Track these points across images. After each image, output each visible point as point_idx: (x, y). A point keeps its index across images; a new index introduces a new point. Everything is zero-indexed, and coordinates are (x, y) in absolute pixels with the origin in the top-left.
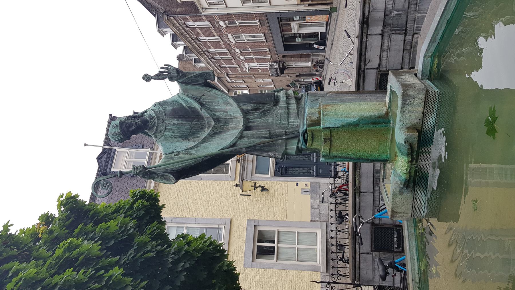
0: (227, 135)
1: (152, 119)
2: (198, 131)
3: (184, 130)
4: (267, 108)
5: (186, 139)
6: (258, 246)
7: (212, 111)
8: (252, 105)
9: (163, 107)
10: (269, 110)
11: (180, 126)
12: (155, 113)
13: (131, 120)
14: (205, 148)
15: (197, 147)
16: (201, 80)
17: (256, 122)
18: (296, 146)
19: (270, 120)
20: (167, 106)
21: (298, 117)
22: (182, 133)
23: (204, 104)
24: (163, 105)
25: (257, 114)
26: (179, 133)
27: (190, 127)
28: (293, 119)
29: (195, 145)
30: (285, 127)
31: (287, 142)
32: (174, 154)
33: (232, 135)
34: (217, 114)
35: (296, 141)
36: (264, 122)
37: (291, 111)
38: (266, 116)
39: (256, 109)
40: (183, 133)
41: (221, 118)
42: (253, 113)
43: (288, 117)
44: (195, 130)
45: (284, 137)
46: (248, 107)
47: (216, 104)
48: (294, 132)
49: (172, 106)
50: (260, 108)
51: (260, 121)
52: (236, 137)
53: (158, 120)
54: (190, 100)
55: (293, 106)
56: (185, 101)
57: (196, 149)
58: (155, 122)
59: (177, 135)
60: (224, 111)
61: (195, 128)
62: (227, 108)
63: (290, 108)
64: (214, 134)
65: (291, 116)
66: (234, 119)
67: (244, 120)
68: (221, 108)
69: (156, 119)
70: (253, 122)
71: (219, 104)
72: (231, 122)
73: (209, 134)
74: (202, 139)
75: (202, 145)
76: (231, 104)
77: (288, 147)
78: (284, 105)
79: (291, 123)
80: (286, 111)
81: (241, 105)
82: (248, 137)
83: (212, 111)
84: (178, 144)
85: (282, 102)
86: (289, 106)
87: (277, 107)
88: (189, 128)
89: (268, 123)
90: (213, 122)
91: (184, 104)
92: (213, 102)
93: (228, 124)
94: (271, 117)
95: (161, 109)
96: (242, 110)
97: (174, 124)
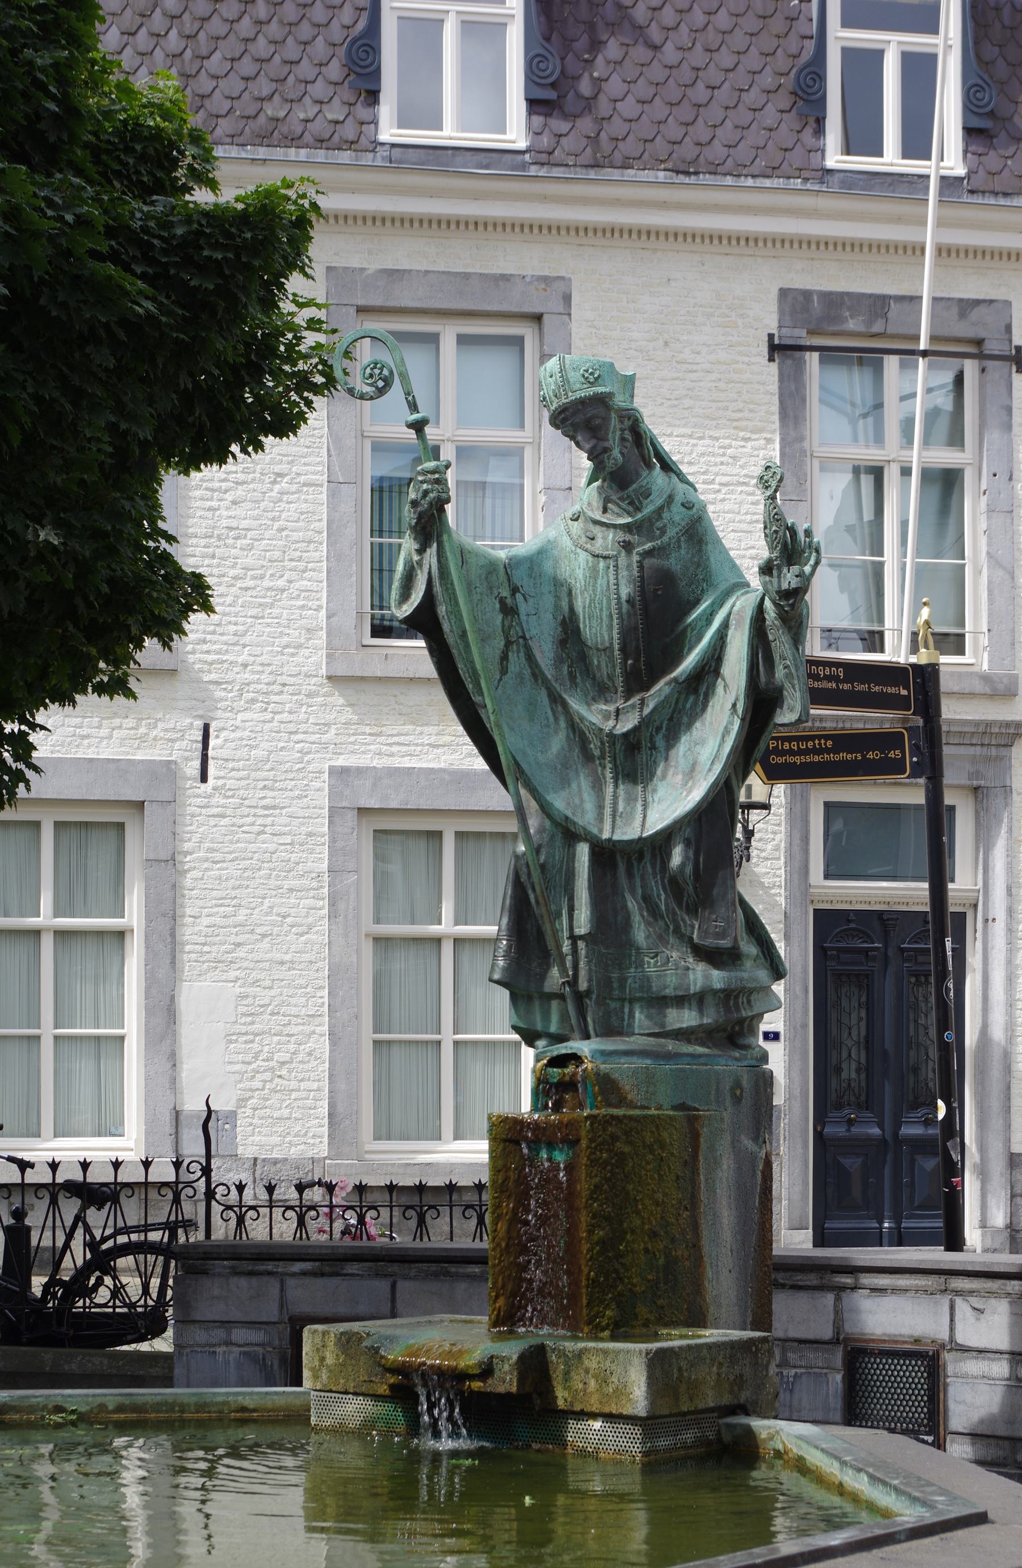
1: (632, 503)
8: (689, 869)
9: (682, 539)
14: (532, 705)
15: (534, 675)
20: (683, 552)
22: (584, 618)
23: (696, 691)
26: (584, 607)
29: (541, 671)
32: (505, 593)
33: (577, 801)
44: (599, 662)
57: (527, 672)
70: (630, 875)
79: (626, 1010)
81: (688, 832)
83: (671, 719)
87: (691, 960)
95: (671, 532)
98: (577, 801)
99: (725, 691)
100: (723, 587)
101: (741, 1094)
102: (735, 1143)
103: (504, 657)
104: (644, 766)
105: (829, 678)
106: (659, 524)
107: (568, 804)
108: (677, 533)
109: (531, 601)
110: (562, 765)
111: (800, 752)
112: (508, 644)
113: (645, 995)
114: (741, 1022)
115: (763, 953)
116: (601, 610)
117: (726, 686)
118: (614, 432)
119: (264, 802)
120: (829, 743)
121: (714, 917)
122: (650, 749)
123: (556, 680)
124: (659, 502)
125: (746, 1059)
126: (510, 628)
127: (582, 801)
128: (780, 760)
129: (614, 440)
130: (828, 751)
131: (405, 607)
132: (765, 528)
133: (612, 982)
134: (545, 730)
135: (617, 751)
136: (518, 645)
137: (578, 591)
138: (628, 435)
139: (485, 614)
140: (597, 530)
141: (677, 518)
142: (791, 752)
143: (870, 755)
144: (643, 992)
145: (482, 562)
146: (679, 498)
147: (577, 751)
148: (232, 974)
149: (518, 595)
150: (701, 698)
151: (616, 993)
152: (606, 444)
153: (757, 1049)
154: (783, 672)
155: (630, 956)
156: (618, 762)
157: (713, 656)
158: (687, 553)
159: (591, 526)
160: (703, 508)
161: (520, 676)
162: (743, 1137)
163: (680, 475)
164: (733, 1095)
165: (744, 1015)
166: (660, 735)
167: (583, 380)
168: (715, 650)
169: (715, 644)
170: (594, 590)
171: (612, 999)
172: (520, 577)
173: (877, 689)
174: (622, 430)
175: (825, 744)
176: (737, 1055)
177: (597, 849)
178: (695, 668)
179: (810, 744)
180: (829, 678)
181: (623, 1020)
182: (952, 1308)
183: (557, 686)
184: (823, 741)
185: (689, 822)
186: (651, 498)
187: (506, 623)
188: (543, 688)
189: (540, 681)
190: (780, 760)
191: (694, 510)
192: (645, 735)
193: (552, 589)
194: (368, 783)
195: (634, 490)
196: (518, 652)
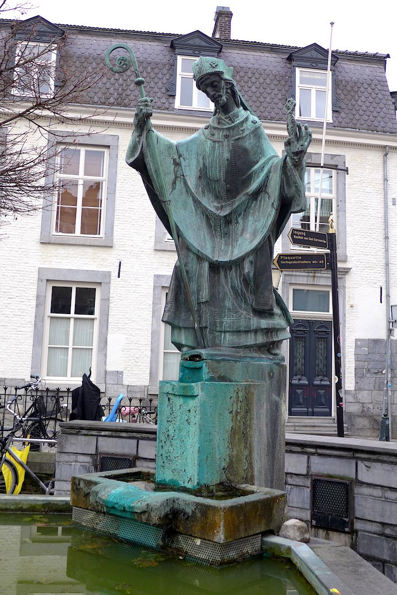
0: (205, 236)
3: (213, 169)
4: (249, 298)
6: (71, 289)
7: (245, 211)
8: (252, 275)
10: (246, 301)
12: (239, 123)
13: (227, 89)
15: (187, 191)
16: (290, 192)
17: (227, 283)
18: (183, 343)
19: (228, 304)
20: (252, 141)
21: (233, 347)
23: (256, 199)
24: (255, 135)
25: (238, 283)
27: (218, 178)
28: (230, 339)
29: (190, 189)
30: (216, 327)
31: (191, 329)
32: (176, 157)
33: (203, 244)
34: (240, 220)
35: (190, 343)
36: (225, 294)
38: (237, 297)
39: (246, 281)
40: (209, 169)
42: (240, 277)
43: (233, 332)
44: (215, 186)
45: (196, 326)
46: (247, 268)
47: (255, 217)
49: (253, 148)
50: (249, 287)
51: (228, 289)
53: (229, 129)
54: (262, 176)
55: (250, 340)
56: (263, 168)
57: (184, 190)
58: (225, 125)
60: (243, 230)
61: (217, 187)
62: (247, 236)
63: (249, 334)
64: (207, 216)
65: (234, 337)
66: (230, 246)
68: (249, 225)
69: (230, 126)
70: (226, 277)
73: (207, 209)
75: (191, 199)
76: (252, 241)
77: (183, 331)
78: (253, 326)
79: (223, 336)
80: (242, 329)
81: (251, 258)
83: (245, 211)
84: (194, 162)
85: (259, 323)
86: (253, 334)
87: (252, 315)
88: (216, 178)
89: (223, 300)
90: (225, 214)
91: (256, 167)
92: (259, 213)
94: (233, 304)
96: (244, 259)
100: (269, 156)
101: (273, 375)
102: (269, 397)
103: (174, 183)
105: (301, 236)
106: (242, 129)
109: (187, 161)
110: (197, 228)
111: (291, 260)
112: (176, 177)
113: (231, 330)
114: (273, 343)
115: (283, 313)
116: (216, 164)
117: (269, 197)
119: (135, 284)
120: (300, 258)
121: (262, 296)
124: (242, 119)
125: (275, 359)
127: (206, 244)
128: (284, 262)
130: (300, 260)
133: (216, 324)
134: (191, 214)
136: (181, 178)
138: (229, 91)
139: (167, 164)
140: (216, 132)
141: (249, 127)
142: (288, 260)
143: (313, 262)
144: (230, 328)
148: (124, 332)
149: (181, 158)
152: (220, 94)
153: (280, 355)
154: (294, 189)
155: (225, 312)
156: (222, 228)
164: (269, 375)
166: (240, 218)
168: (265, 182)
171: (216, 331)
172: (182, 150)
173: (316, 240)
174: (227, 89)
176: (271, 358)
177: (211, 266)
178: (256, 189)
179: (294, 258)
180: (301, 236)
182: (357, 463)
183: (197, 196)
185: (252, 254)
187: (176, 169)
189: (189, 194)
190: (284, 262)
192: (234, 217)
193: (196, 156)
194: (165, 280)
196: (180, 181)
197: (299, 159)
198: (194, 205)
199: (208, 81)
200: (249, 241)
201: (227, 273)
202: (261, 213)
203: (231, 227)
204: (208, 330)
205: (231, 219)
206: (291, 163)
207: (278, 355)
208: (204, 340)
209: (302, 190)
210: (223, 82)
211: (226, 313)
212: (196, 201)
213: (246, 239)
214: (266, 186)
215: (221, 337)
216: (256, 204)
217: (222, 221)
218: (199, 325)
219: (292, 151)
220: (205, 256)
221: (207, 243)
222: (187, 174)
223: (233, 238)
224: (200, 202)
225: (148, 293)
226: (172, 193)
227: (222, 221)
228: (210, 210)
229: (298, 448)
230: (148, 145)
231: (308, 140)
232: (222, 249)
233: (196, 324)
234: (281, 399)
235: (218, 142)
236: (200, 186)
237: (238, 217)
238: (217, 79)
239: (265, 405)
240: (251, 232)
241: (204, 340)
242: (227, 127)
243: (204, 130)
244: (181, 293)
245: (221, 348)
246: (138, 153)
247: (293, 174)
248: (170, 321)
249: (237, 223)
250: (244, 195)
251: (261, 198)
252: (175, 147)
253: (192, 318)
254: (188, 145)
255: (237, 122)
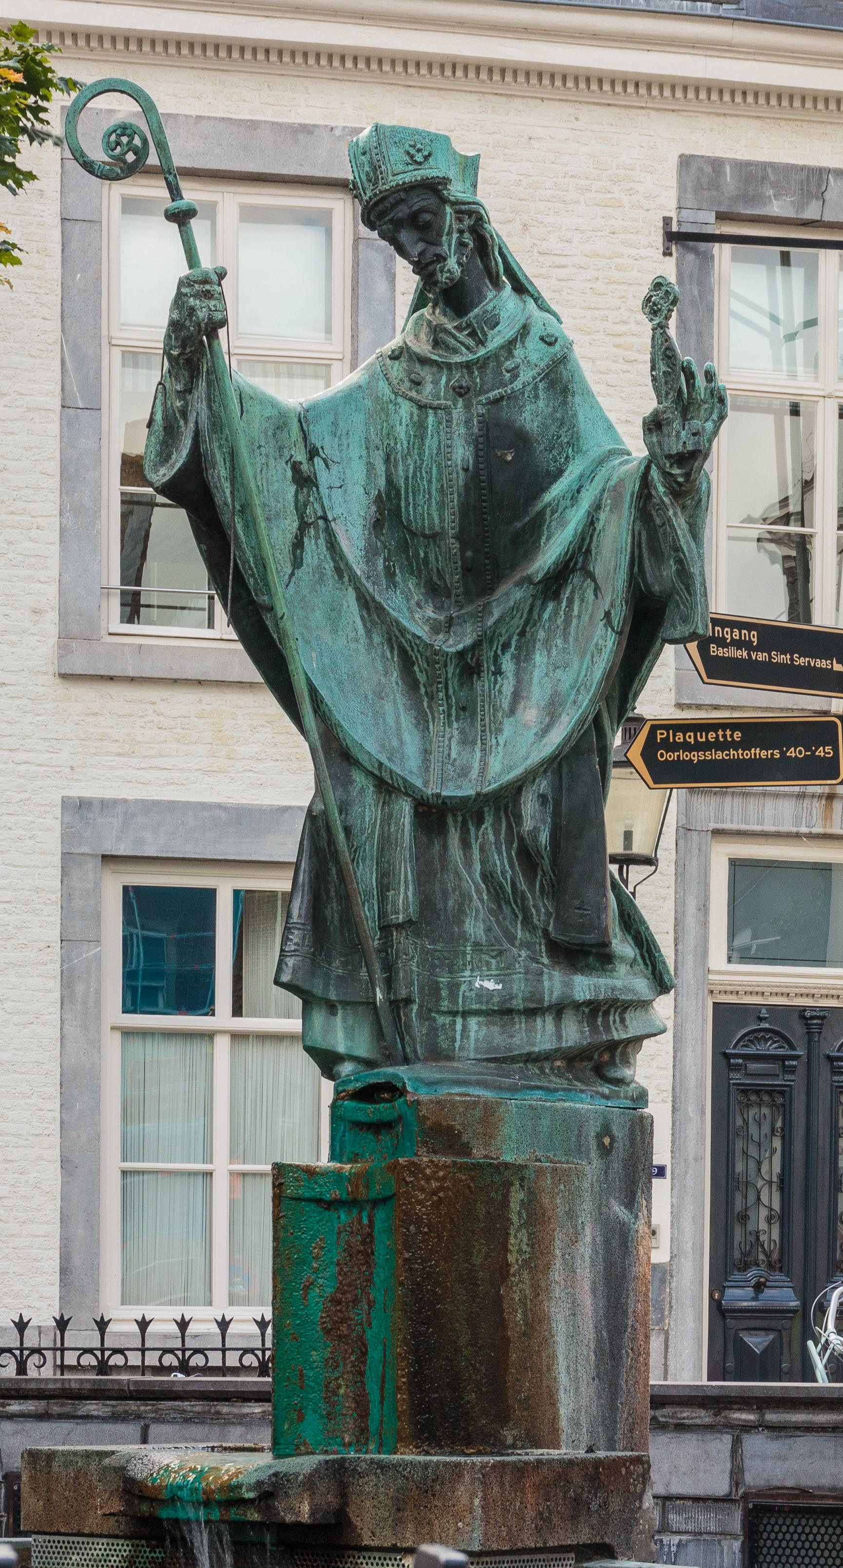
1: (473, 334)
2: (420, 572)
3: (420, 500)
4: (538, 911)
5: (380, 510)
7: (522, 634)
8: (544, 837)
10: (527, 921)
11: (439, 480)
14: (334, 613)
15: (338, 571)
18: (341, 1049)
20: (541, 403)
21: (489, 1060)
22: (407, 492)
23: (556, 596)
25: (502, 863)
26: (407, 478)
27: (437, 529)
29: (347, 564)
30: (439, 998)
31: (360, 1008)
32: (300, 456)
33: (395, 743)
34: (508, 664)
35: (363, 1050)
36: (465, 897)
37: (520, 1025)
38: (500, 907)
41: (482, 685)
42: (509, 843)
44: (426, 553)
45: (379, 996)
47: (554, 652)
48: (407, 1038)
50: (536, 875)
52: (381, 764)
53: (468, 366)
54: (575, 518)
56: (575, 495)
57: (329, 566)
58: (455, 351)
59: (401, 468)
60: (516, 696)
63: (539, 1021)
64: (403, 653)
65: (495, 1029)
67: (468, 798)
68: (535, 680)
69: (471, 357)
70: (466, 844)
71: (556, 667)
72: (462, 732)
73: (403, 631)
74: (377, 597)
75: (351, 595)
79: (459, 1027)
81: (543, 785)
82: (388, 819)
83: (522, 634)
85: (568, 985)
87: (545, 960)
90: (460, 647)
93: (457, 720)
94: (488, 930)
95: (526, 376)
97: (444, 451)
98: (395, 743)
99: (596, 595)
100: (595, 453)
101: (611, 1144)
103: (298, 544)
104: (487, 699)
106: (509, 364)
107: (383, 746)
108: (534, 378)
109: (334, 468)
110: (374, 692)
111: (698, 747)
112: (303, 526)
113: (484, 1007)
114: (612, 1046)
117: (597, 589)
118: (450, 233)
120: (737, 736)
121: (577, 903)
122: (494, 674)
123: (368, 578)
126: (305, 506)
128: (671, 756)
129: (450, 246)
130: (735, 745)
131: (162, 471)
132: (653, 368)
133: (440, 989)
134: (353, 645)
135: (450, 675)
136: (317, 528)
137: (399, 456)
138: (468, 238)
139: (272, 485)
140: (426, 374)
141: (534, 357)
142: (686, 747)
143: (792, 753)
144: (481, 1003)
145: (269, 412)
146: (536, 331)
147: (395, 675)
149: (316, 459)
150: (564, 605)
151: (445, 1004)
152: (438, 250)
153: (633, 1085)
154: (674, 568)
155: (464, 953)
156: (451, 691)
157: (580, 548)
158: (547, 406)
159: (418, 367)
160: (569, 345)
161: (319, 570)
162: (613, 1201)
163: (537, 299)
164: (600, 1145)
165: (616, 1037)
166: (508, 656)
167: (408, 159)
168: (583, 539)
169: (583, 532)
170: (420, 454)
172: (320, 435)
173: (802, 661)
175: (732, 736)
176: (606, 1091)
178: (556, 564)
179: (712, 736)
180: (738, 644)
181: (454, 1040)
183: (369, 586)
184: (728, 733)
185: (545, 771)
186: (498, 328)
188: (350, 589)
189: (346, 579)
190: (671, 756)
191: (557, 347)
192: (487, 654)
193: (364, 453)
194: (117, 823)
195: (476, 317)
196: (317, 537)
197: (687, 475)
198: (362, 617)
199: (403, 211)
200: (534, 730)
201: (468, 830)
202: (571, 639)
203: (478, 685)
204: (415, 1007)
205: (478, 660)
206: (665, 486)
207: (628, 1084)
208: (402, 1039)
209: (697, 573)
210: (448, 210)
211: (469, 957)
212: (366, 603)
213: (526, 727)
214: (588, 551)
215: (454, 1030)
216: (556, 613)
217: (451, 669)
218: (389, 993)
219: (667, 452)
220: (401, 782)
221: (407, 737)
222: (338, 511)
223: (487, 720)
224: (380, 609)
225: (37, 890)
226: (293, 579)
227: (451, 669)
228: (414, 635)
229: (702, 1413)
230: (214, 424)
231: (715, 416)
232: (454, 755)
233: (378, 990)
234: (636, 1217)
235: (436, 408)
236: (376, 553)
237: (499, 652)
238: (430, 201)
239: (588, 1231)
240: (543, 704)
241: (402, 1039)
242: (464, 359)
243: (388, 361)
244: (328, 897)
245: (455, 1064)
246: (185, 452)
247: (669, 520)
248: (299, 983)
249: (498, 672)
250: (519, 584)
251: (573, 592)
252: (295, 426)
253: (363, 974)
254: (336, 415)
255: (495, 340)
